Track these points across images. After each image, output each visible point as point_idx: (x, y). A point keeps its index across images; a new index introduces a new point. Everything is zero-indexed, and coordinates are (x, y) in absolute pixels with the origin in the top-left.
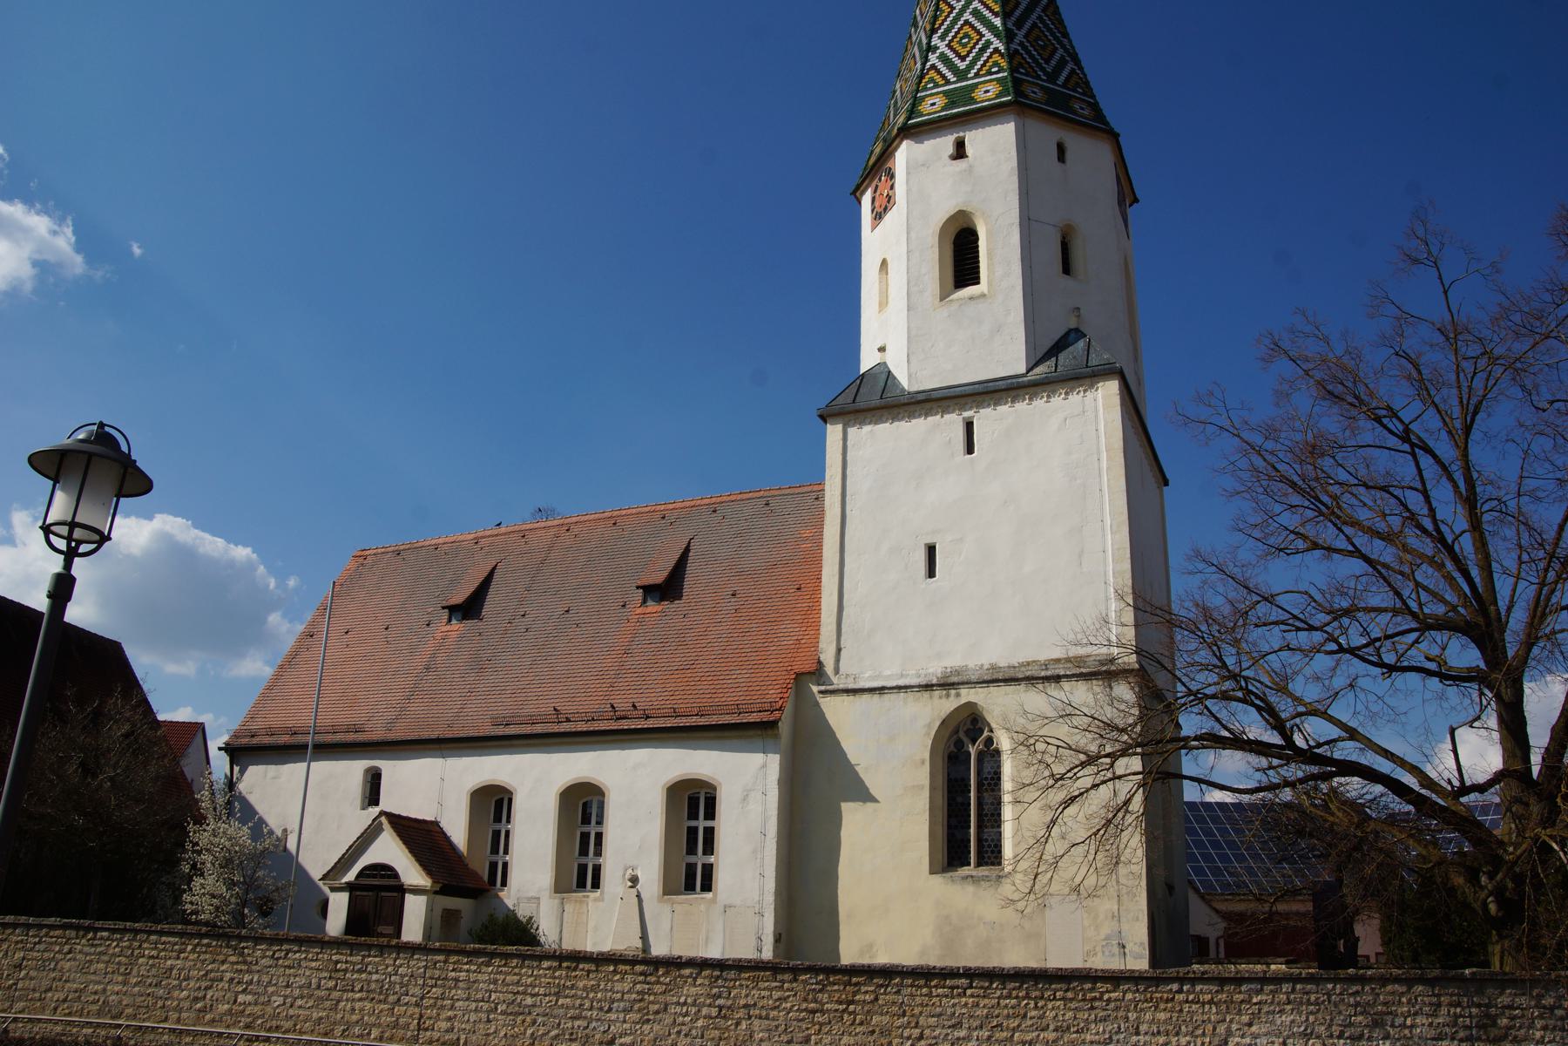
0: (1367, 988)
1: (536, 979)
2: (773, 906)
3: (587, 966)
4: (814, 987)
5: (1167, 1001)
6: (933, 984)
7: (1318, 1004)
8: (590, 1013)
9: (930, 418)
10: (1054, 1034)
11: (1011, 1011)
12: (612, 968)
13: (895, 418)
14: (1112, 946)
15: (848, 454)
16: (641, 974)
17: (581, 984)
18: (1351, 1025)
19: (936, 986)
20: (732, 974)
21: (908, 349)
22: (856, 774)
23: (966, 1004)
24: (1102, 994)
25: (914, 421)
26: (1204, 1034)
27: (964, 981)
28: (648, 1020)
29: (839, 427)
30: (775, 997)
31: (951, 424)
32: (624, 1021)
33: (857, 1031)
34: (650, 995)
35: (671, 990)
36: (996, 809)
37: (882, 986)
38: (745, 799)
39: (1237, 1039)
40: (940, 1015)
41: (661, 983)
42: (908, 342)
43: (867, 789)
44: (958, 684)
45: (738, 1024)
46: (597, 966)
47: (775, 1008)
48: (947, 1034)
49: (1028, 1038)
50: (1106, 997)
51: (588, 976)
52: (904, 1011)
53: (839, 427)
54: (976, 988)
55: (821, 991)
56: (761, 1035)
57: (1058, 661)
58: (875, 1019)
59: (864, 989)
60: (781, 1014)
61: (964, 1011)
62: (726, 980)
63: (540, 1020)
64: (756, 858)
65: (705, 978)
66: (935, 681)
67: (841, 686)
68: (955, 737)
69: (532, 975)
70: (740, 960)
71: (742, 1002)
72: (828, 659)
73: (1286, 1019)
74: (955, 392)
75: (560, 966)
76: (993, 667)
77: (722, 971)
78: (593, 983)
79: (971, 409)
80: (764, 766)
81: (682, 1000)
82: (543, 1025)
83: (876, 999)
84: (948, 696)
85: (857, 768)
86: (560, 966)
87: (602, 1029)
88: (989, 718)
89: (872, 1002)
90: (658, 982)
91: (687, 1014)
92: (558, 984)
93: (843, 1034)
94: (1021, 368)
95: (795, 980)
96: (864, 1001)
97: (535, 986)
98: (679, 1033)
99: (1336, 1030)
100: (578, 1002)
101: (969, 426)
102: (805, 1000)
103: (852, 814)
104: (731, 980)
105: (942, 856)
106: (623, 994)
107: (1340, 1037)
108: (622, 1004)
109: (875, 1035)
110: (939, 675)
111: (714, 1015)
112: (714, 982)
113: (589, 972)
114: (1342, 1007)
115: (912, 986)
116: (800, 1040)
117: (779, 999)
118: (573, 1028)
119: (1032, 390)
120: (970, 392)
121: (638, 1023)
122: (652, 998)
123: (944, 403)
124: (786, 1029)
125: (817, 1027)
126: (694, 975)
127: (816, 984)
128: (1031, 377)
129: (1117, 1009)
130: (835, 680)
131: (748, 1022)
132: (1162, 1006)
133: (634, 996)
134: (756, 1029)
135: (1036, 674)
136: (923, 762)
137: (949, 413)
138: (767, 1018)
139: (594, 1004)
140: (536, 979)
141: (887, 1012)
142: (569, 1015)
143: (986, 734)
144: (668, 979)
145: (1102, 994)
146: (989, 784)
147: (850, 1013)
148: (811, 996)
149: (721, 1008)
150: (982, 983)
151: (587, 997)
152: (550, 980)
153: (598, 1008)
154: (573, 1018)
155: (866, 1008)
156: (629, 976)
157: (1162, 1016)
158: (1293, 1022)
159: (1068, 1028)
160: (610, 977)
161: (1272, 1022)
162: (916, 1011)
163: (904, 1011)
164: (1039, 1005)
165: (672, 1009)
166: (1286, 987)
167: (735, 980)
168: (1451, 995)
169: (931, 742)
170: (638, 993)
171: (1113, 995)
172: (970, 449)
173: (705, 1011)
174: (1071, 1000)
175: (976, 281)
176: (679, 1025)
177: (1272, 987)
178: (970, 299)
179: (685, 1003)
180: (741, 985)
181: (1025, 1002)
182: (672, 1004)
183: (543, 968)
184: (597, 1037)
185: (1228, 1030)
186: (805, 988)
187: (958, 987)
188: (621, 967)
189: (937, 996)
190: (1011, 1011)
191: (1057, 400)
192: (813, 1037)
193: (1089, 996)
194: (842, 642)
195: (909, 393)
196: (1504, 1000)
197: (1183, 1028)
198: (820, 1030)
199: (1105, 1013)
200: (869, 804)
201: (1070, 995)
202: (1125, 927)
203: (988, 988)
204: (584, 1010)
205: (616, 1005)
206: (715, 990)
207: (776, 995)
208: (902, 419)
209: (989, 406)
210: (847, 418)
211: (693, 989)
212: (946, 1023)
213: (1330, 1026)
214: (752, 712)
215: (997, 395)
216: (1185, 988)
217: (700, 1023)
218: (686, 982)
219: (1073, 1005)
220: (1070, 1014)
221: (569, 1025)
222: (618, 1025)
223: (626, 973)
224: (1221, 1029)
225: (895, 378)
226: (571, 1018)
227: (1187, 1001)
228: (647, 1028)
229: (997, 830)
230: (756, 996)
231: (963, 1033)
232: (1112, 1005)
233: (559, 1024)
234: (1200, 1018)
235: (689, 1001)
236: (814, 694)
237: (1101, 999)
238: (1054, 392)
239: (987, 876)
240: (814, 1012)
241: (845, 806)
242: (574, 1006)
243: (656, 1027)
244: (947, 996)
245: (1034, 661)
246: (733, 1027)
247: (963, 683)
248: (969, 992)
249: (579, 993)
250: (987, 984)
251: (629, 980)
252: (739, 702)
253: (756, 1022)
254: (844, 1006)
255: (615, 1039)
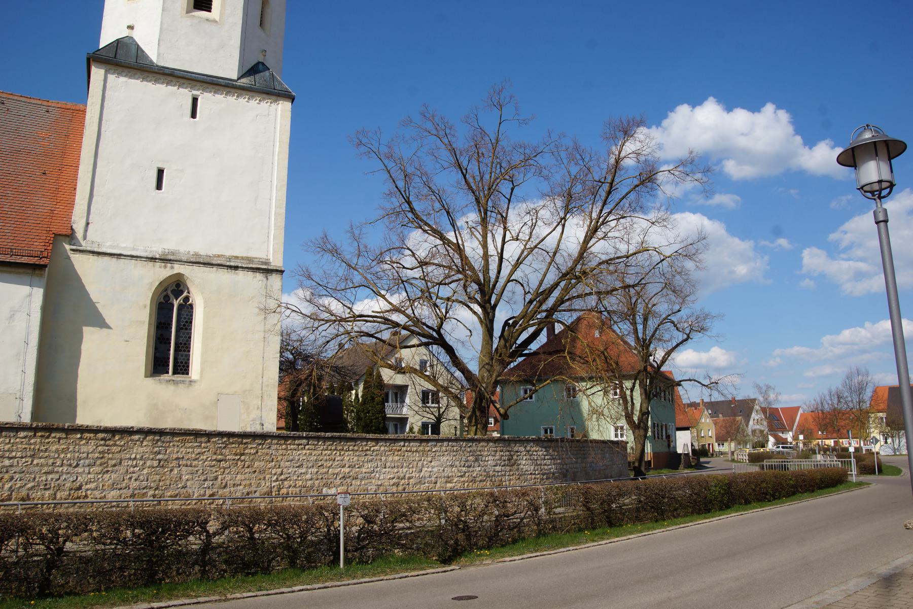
0: (474, 444)
1: (13, 446)
2: (32, 394)
3: (58, 435)
4: (220, 445)
5: (399, 451)
6: (288, 443)
7: (457, 451)
8: (61, 469)
9: (169, 87)
10: (348, 469)
11: (328, 457)
12: (79, 436)
13: (144, 79)
14: (256, 424)
15: (107, 92)
16: (102, 439)
17: (54, 448)
18: (467, 461)
19: (290, 444)
20: (168, 438)
21: (160, 36)
22: (96, 308)
23: (306, 454)
24: (370, 447)
25: (158, 85)
26: (413, 467)
27: (304, 441)
28: (108, 471)
29: (102, 71)
30: (197, 452)
31: (184, 95)
32: (89, 473)
33: (246, 471)
34: (109, 454)
35: (124, 450)
36: (187, 341)
37: (260, 444)
38: (12, 317)
39: (426, 469)
40: (292, 460)
41: (117, 446)
42: (160, 31)
43: (104, 320)
44: (173, 261)
45: (171, 471)
46: (67, 434)
47: (196, 459)
48: (296, 471)
49: (336, 472)
50: (372, 449)
51: (59, 442)
52: (273, 459)
53: (102, 71)
54: (310, 445)
55: (224, 448)
56: (187, 477)
57: (237, 257)
58: (257, 464)
59: (250, 446)
60: (200, 463)
61: (304, 458)
62: (163, 442)
63: (17, 476)
64: (19, 360)
65: (149, 441)
66: (157, 256)
67: (89, 249)
68: (165, 293)
69: (9, 443)
70: (174, 429)
71: (175, 456)
72: (79, 228)
73: (445, 458)
74: (191, 76)
75: (35, 435)
76: (196, 254)
77: (160, 436)
78: (63, 447)
79: (198, 90)
80: (30, 295)
81: (133, 456)
82: (20, 480)
83: (257, 452)
84: (165, 267)
85: (97, 305)
86: (35, 435)
87: (71, 479)
88: (189, 285)
89: (254, 454)
90: (115, 445)
91: (136, 466)
92: (34, 449)
93: (237, 474)
94: (234, 76)
95: (209, 441)
96: (250, 453)
97: (13, 451)
98: (130, 478)
99: (462, 464)
100: (51, 461)
101: (195, 100)
102: (215, 454)
103: (90, 336)
104: (167, 442)
105: (151, 367)
106: (88, 454)
107: (464, 467)
108: (87, 462)
109: (256, 474)
110: (160, 253)
111: (155, 465)
112: (155, 444)
113: (60, 439)
114: (465, 453)
115: (277, 444)
116: (212, 479)
117: (199, 453)
118: (46, 480)
119: (240, 91)
120: (201, 80)
121: (100, 473)
122: (110, 456)
123: (182, 81)
124: (203, 473)
125: (222, 470)
126: (141, 440)
127: (222, 443)
128: (239, 83)
129: (377, 455)
130: (83, 243)
131: (179, 469)
132: (396, 453)
133: (97, 455)
134: (184, 473)
135: (224, 263)
136: (145, 307)
137: (183, 88)
138: (191, 466)
139: (65, 462)
140: (13, 446)
141: (263, 460)
142: (43, 472)
143: (185, 294)
144: (123, 443)
145: (370, 447)
146: (184, 325)
147: (242, 461)
148: (218, 451)
149: (160, 461)
150: (314, 442)
151: (58, 457)
152: (26, 446)
153: (68, 465)
154: (47, 473)
155: (251, 458)
156: (93, 441)
157: (396, 458)
158: (447, 460)
159: (355, 466)
160: (77, 442)
161: (440, 460)
162: (279, 459)
163: (273, 459)
164: (342, 454)
165: (125, 463)
166: (445, 443)
167: (170, 442)
168: (501, 447)
169: (151, 294)
170: (100, 452)
171: (376, 448)
172: (194, 115)
173: (149, 463)
174: (357, 450)
175: (209, 9)
176: (130, 473)
177: (440, 444)
178: (207, 20)
179: (135, 458)
180: (174, 445)
181: (335, 452)
182: (126, 459)
183: (19, 438)
184: (68, 485)
185: (423, 466)
186: (215, 446)
187: (301, 445)
188: (87, 435)
189: (291, 450)
190: (328, 457)
191: (254, 103)
192: (220, 477)
193: (364, 449)
194: (90, 219)
195: (157, 66)
196: (516, 449)
197: (405, 464)
198: (224, 472)
199: (372, 457)
200: (104, 330)
201: (356, 448)
202: (264, 414)
203: (317, 445)
204: (56, 467)
205: (82, 462)
206: (156, 449)
207: (197, 451)
208: (150, 81)
209: (210, 92)
210: (108, 67)
211: (141, 450)
212: (295, 465)
213: (461, 461)
214: (23, 256)
215: (217, 87)
216: (406, 444)
217: (145, 471)
218: (135, 444)
219: (357, 453)
220: (356, 458)
221: (44, 478)
222: (84, 476)
223: (90, 439)
224: (420, 464)
225: (143, 51)
226: (44, 473)
227: (407, 451)
228: (107, 476)
229: (187, 353)
230: (184, 452)
231: (303, 470)
232: (375, 453)
233: (35, 479)
234: (412, 459)
235: (138, 457)
236: (66, 250)
237: (370, 450)
238: (253, 97)
239: (183, 381)
240: (220, 461)
241: (86, 330)
242: (47, 464)
243: (113, 476)
244: (295, 450)
245: (222, 255)
246: (168, 473)
247: (176, 261)
248: (307, 447)
249: (52, 454)
250: (316, 443)
251: (93, 444)
252: (13, 247)
253: (184, 469)
254: (239, 457)
255: (82, 486)
